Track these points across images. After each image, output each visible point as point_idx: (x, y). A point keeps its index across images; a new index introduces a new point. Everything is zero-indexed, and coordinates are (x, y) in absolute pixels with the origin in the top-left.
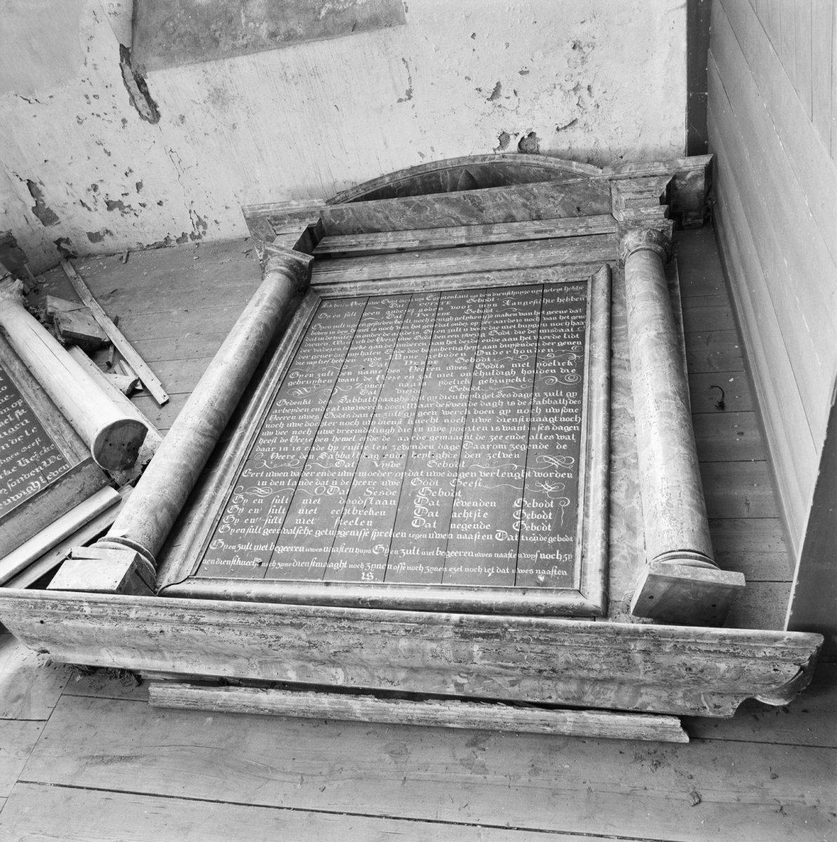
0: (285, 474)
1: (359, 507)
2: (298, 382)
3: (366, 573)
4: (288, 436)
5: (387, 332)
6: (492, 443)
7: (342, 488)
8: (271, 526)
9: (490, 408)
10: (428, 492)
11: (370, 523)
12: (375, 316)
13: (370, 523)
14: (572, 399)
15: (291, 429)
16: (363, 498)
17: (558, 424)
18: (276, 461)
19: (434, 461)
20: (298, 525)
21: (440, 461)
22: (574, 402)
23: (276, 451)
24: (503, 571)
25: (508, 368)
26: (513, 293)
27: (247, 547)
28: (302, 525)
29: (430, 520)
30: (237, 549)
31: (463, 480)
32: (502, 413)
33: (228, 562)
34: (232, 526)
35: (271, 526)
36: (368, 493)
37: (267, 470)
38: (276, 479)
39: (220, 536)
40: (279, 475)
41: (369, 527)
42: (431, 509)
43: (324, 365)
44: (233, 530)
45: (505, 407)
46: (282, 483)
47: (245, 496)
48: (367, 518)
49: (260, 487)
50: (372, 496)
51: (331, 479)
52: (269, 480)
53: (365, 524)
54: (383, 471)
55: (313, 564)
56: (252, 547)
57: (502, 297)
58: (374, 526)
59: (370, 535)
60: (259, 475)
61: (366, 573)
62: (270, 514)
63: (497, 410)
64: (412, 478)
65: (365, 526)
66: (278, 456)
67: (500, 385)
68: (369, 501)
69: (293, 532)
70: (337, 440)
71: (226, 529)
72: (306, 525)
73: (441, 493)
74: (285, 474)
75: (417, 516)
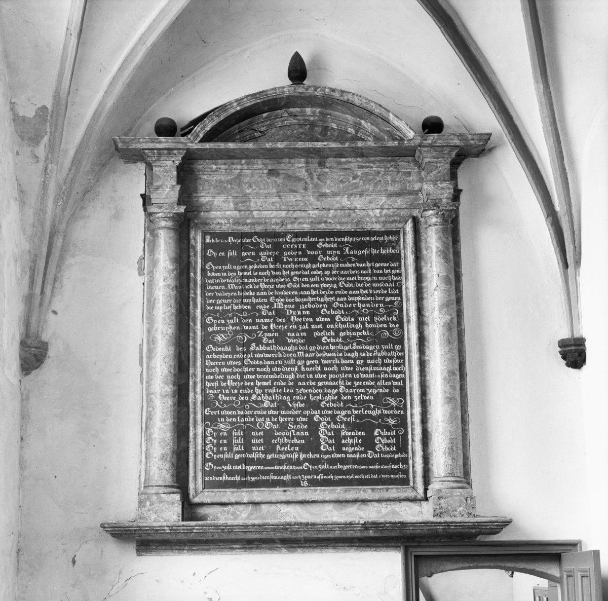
0: (234, 413)
1: (288, 437)
2: (216, 328)
3: (303, 481)
4: (225, 380)
5: (266, 277)
6: (356, 388)
7: (274, 423)
8: (238, 452)
9: (350, 358)
10: (325, 426)
11: (297, 449)
12: (251, 257)
13: (297, 449)
14: (398, 351)
15: (225, 374)
16: (289, 431)
17: (393, 372)
18: (225, 402)
19: (324, 402)
20: (255, 451)
21: (328, 402)
22: (400, 354)
23: (221, 393)
24: (375, 477)
25: (356, 322)
26: (350, 239)
27: (229, 467)
28: (256, 451)
29: (331, 445)
30: (223, 469)
31: (344, 416)
32: (358, 362)
33: (221, 478)
34: (214, 453)
35: (238, 452)
36: (291, 427)
37: (221, 410)
38: (230, 416)
39: (209, 460)
40: (230, 413)
41: (297, 451)
42: (330, 437)
43: (228, 311)
44: (215, 456)
45: (360, 358)
46: (234, 420)
47: (213, 430)
48: (295, 445)
49: (221, 423)
50: (293, 429)
51: (265, 416)
52: (224, 416)
53: (294, 449)
54: (295, 410)
55: (272, 477)
56: (232, 467)
57: (343, 243)
58: (300, 450)
59: (299, 456)
60: (217, 413)
61: (303, 481)
62: (235, 444)
63: (355, 359)
64: (314, 415)
65: (295, 451)
66: (224, 398)
67: (354, 337)
68: (292, 433)
69: (252, 456)
70: (259, 384)
71: (210, 455)
72: (259, 451)
73: (333, 426)
74: (234, 413)
75: (323, 443)
